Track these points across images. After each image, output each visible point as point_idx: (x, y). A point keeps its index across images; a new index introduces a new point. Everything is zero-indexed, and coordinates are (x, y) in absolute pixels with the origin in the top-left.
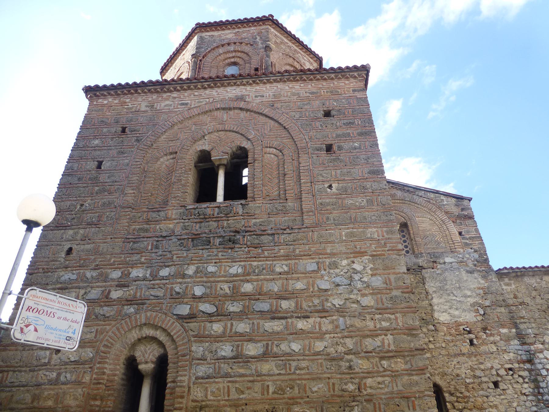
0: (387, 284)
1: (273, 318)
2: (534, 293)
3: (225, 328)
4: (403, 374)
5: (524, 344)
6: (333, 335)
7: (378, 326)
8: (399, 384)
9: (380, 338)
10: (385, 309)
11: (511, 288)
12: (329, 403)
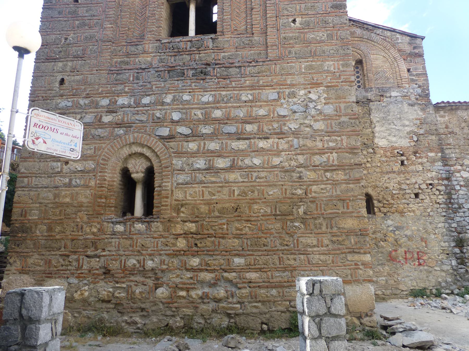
0: (337, 112)
1: (239, 139)
2: (463, 124)
3: (199, 146)
4: (342, 183)
5: (446, 165)
6: (288, 153)
7: (326, 146)
8: (338, 190)
9: (326, 155)
10: (333, 132)
11: (444, 119)
12: (282, 203)
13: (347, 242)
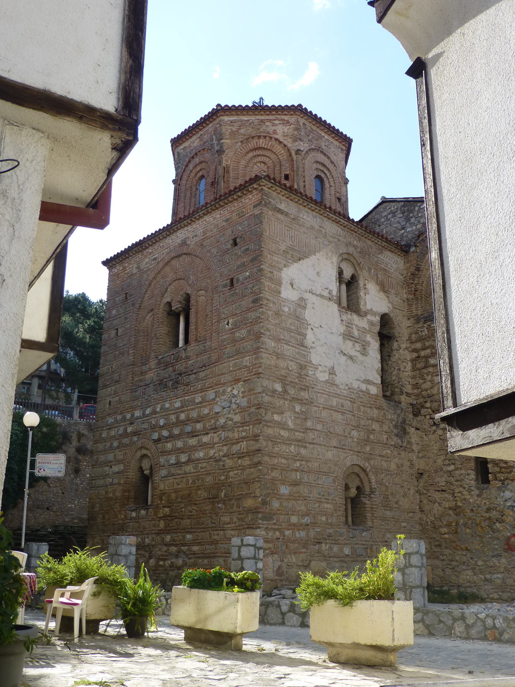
1: (193, 436)
13: (246, 520)
